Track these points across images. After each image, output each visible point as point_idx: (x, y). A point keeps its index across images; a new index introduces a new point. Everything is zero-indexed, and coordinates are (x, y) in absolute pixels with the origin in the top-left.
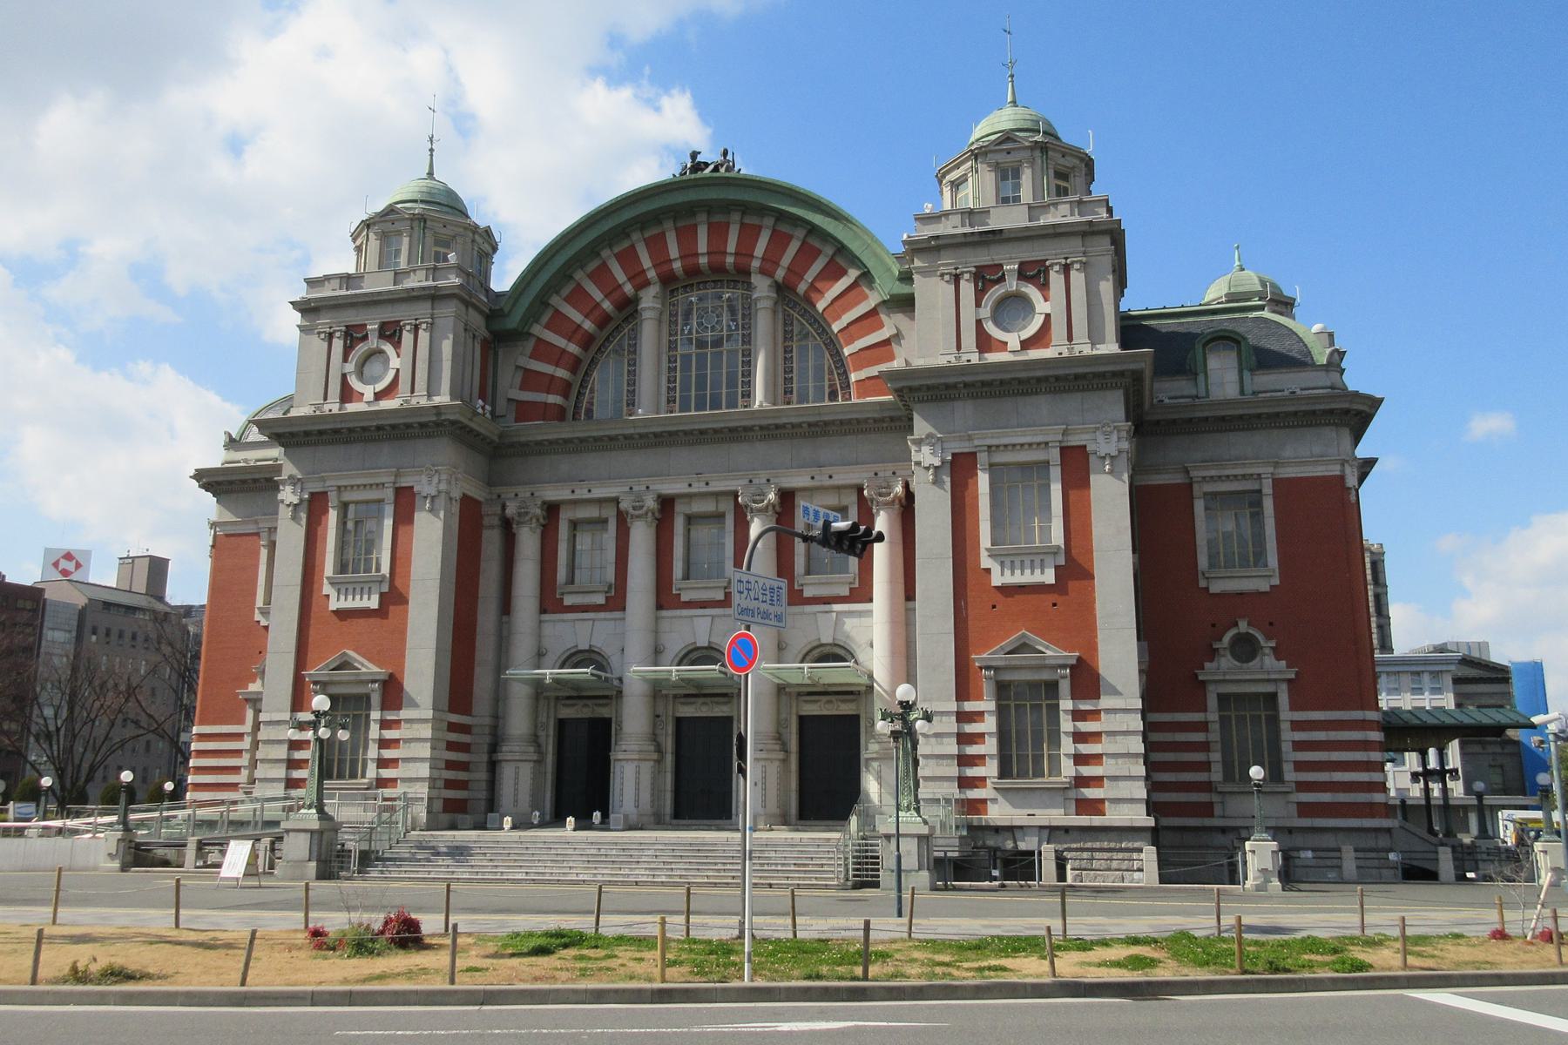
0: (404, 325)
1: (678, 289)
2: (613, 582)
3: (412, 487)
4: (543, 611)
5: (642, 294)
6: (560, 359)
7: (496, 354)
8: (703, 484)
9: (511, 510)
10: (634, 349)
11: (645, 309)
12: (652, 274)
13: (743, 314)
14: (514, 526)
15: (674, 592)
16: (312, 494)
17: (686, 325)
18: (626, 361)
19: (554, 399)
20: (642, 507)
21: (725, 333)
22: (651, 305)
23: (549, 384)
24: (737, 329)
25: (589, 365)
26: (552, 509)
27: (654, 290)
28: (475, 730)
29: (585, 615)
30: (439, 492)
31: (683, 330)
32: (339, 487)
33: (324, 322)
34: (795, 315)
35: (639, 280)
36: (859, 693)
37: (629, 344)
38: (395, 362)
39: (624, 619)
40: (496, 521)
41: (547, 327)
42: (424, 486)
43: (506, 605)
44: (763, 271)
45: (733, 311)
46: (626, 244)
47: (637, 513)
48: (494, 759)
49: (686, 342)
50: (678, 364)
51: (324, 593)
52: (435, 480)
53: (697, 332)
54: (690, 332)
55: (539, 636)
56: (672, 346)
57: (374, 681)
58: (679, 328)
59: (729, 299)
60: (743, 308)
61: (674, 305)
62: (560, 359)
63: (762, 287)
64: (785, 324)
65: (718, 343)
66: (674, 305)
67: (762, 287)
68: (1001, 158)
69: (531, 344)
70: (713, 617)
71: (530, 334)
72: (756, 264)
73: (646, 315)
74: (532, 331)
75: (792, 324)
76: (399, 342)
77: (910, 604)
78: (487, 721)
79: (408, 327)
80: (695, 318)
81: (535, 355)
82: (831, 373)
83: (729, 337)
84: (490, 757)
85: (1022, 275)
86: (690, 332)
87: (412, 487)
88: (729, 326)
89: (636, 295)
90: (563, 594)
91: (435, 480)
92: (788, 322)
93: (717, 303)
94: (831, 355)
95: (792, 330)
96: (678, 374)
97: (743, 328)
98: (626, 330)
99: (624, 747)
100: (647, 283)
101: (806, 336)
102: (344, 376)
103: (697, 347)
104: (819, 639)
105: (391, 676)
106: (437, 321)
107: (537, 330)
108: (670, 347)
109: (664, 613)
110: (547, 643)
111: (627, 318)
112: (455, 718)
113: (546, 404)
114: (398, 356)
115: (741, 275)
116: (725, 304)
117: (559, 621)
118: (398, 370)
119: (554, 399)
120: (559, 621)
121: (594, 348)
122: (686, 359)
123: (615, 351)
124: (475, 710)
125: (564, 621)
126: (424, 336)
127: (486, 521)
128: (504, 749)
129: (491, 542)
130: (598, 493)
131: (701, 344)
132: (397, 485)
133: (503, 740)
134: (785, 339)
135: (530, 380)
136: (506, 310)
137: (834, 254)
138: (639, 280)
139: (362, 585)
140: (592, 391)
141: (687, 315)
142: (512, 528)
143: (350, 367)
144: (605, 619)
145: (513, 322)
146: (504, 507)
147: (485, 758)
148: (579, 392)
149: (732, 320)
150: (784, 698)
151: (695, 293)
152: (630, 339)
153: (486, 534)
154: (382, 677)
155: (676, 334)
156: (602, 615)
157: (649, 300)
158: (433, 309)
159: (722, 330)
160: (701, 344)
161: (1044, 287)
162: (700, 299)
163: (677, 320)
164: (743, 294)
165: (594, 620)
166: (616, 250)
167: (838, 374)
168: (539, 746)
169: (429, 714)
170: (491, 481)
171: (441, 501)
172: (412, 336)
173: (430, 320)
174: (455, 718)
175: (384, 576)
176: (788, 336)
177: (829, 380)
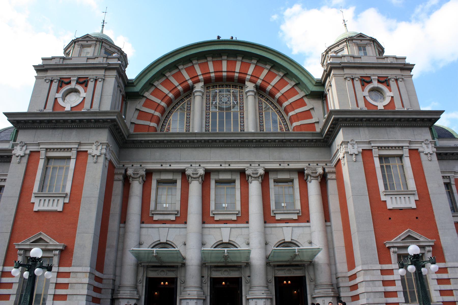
0: (90, 79)
1: (210, 86)
2: (179, 210)
3: (87, 151)
4: (142, 222)
5: (196, 85)
6: (156, 108)
7: (126, 104)
8: (227, 165)
9: (130, 172)
10: (189, 109)
11: (196, 92)
12: (201, 77)
13: (240, 99)
14: (131, 180)
15: (211, 215)
16: (31, 152)
18: (186, 113)
19: (153, 124)
20: (197, 174)
22: (200, 90)
23: (151, 117)
25: (168, 114)
26: (149, 173)
27: (201, 84)
28: (104, 281)
29: (164, 225)
30: (101, 154)
31: (212, 103)
32: (47, 149)
33: (50, 74)
34: (263, 100)
35: (195, 79)
36: (304, 265)
37: (187, 107)
38: (83, 94)
39: (186, 228)
40: (121, 177)
41: (151, 94)
42: (93, 150)
43: (124, 219)
44: (250, 81)
45: (235, 96)
46: (190, 65)
47: (195, 176)
48: (114, 297)
49: (214, 107)
50: (210, 116)
51: (31, 202)
52: (100, 148)
53: (219, 104)
54: (216, 103)
55: (140, 235)
56: (208, 108)
57: (56, 250)
58: (211, 102)
59: (233, 92)
60: (240, 96)
61: (208, 93)
62: (156, 108)
63: (250, 86)
64: (259, 104)
65: (229, 109)
66: (208, 93)
67: (250, 86)
68: (359, 42)
69: (144, 100)
70: (231, 228)
71: (143, 96)
72: (248, 77)
73: (196, 94)
74: (145, 95)
75: (262, 104)
76: (86, 86)
77: (328, 224)
78: (112, 276)
79: (92, 80)
80: (218, 98)
81: (144, 105)
82: (280, 124)
83: (234, 107)
84: (112, 296)
85: (379, 82)
86: (216, 103)
87: (87, 151)
89: (193, 86)
90: (153, 214)
91: (100, 148)
92: (260, 103)
93: (228, 93)
94: (280, 117)
95: (262, 106)
96: (210, 120)
97: (240, 104)
98: (186, 101)
99: (188, 292)
100: (199, 81)
101: (269, 108)
102: (56, 99)
103: (219, 110)
104: (284, 240)
105: (66, 247)
106: (107, 79)
107: (147, 94)
108: (206, 109)
109: (206, 225)
110: (143, 239)
111: (186, 96)
112: (98, 274)
113: (149, 126)
114: (85, 92)
115: (241, 82)
116: (231, 94)
117: (150, 228)
118: (84, 98)
119: (153, 124)
120: (150, 228)
121: (171, 107)
123: (181, 109)
124: (105, 271)
125: (153, 228)
126: (99, 84)
127: (116, 177)
128: (121, 292)
129: (118, 187)
130: (174, 167)
132: (79, 150)
133: (119, 287)
134: (259, 109)
135: (142, 115)
136: (135, 84)
137: (283, 76)
138: (195, 79)
139: (54, 198)
140: (169, 124)
141: (214, 97)
142: (129, 181)
143: (59, 95)
144: (175, 228)
145: (137, 88)
146: (126, 171)
147: (110, 297)
148: (163, 125)
149: (235, 101)
150: (269, 268)
151: (218, 89)
152: (187, 104)
153: (115, 183)
154: (61, 248)
155: (209, 104)
156: (173, 225)
157: (199, 87)
158: (105, 73)
160: (221, 109)
161: (388, 86)
162: (220, 91)
163: (209, 99)
164: (239, 91)
165: (169, 228)
166: (185, 67)
167: (284, 125)
168: (138, 291)
169: (88, 269)
170: (120, 157)
171: (101, 159)
172: (93, 83)
173: (103, 78)
174: (98, 274)
175: (67, 194)
176: (260, 108)
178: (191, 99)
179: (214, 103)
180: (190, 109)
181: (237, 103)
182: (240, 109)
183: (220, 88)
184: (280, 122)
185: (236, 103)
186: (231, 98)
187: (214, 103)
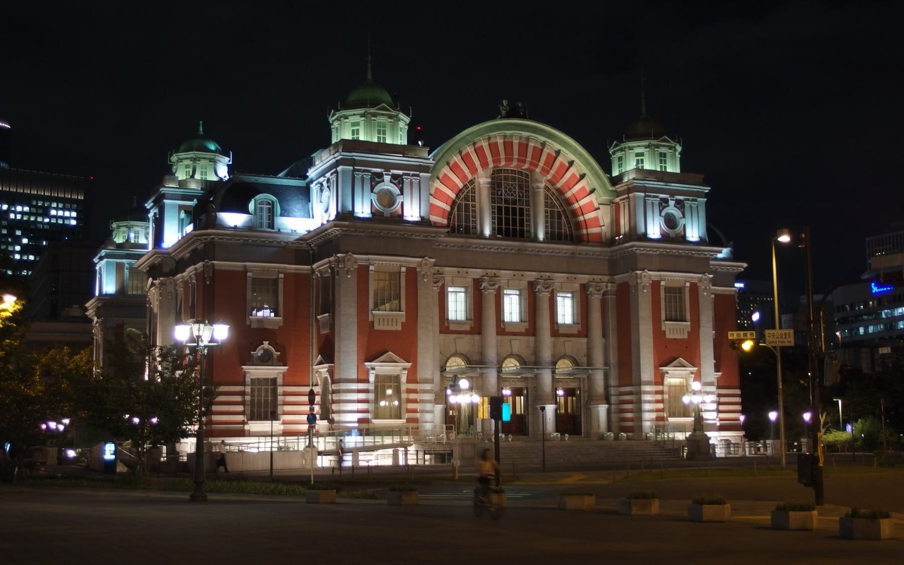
13: (526, 190)
17: (498, 191)
21: (517, 198)
24: (523, 197)
45: (521, 187)
53: (505, 196)
54: (501, 195)
75: (547, 199)
82: (565, 226)
88: (519, 196)
97: (526, 197)
122: (500, 208)
131: (507, 201)
149: (521, 192)
159: (516, 197)
163: (495, 188)
177: (564, 229)
178: (475, 186)
179: (499, 194)
180: (475, 200)
181: (523, 195)
182: (526, 204)
183: (505, 173)
184: (564, 222)
185: (521, 196)
186: (517, 188)
187: (499, 194)
